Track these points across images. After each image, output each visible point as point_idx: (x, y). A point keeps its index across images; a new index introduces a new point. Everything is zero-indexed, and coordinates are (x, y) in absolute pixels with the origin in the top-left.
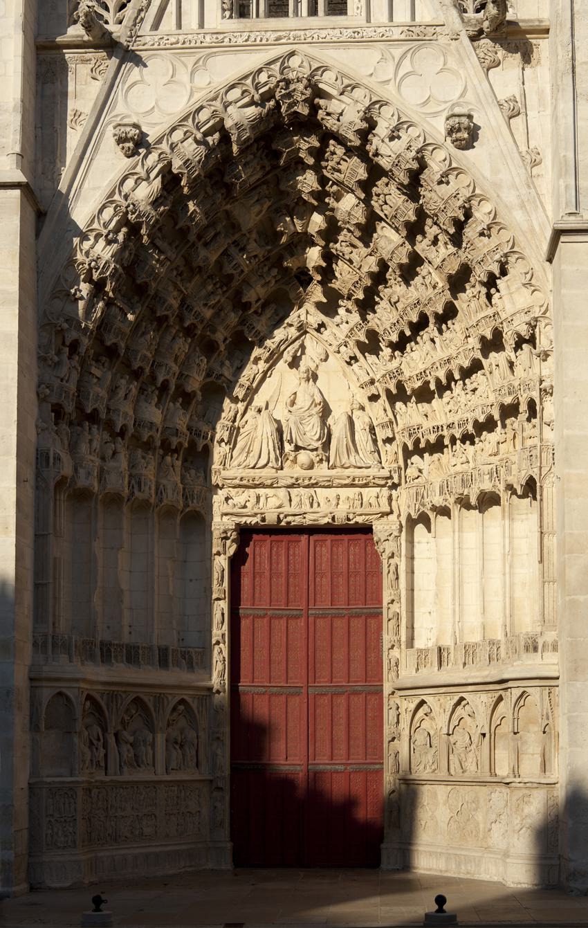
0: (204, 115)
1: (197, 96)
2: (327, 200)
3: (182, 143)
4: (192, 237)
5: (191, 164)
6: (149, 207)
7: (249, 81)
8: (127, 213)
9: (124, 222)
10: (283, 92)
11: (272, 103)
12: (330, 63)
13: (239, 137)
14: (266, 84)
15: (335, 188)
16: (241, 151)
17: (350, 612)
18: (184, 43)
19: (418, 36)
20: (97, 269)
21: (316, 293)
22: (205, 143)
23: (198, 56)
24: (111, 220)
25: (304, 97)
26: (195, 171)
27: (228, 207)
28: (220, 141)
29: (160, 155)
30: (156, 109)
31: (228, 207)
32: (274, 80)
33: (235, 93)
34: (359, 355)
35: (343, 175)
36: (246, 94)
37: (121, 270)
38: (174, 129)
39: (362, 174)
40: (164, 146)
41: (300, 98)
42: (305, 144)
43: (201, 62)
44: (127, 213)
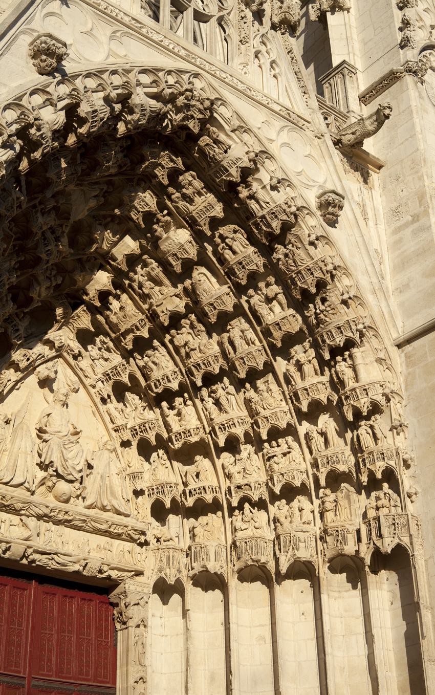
1: (111, 60)
3: (93, 92)
5: (96, 116)
6: (49, 134)
9: (22, 133)
15: (168, 218)
17: (78, 688)
21: (83, 320)
25: (201, 116)
26: (95, 126)
29: (73, 90)
34: (113, 397)
36: (154, 85)
42: (166, 161)
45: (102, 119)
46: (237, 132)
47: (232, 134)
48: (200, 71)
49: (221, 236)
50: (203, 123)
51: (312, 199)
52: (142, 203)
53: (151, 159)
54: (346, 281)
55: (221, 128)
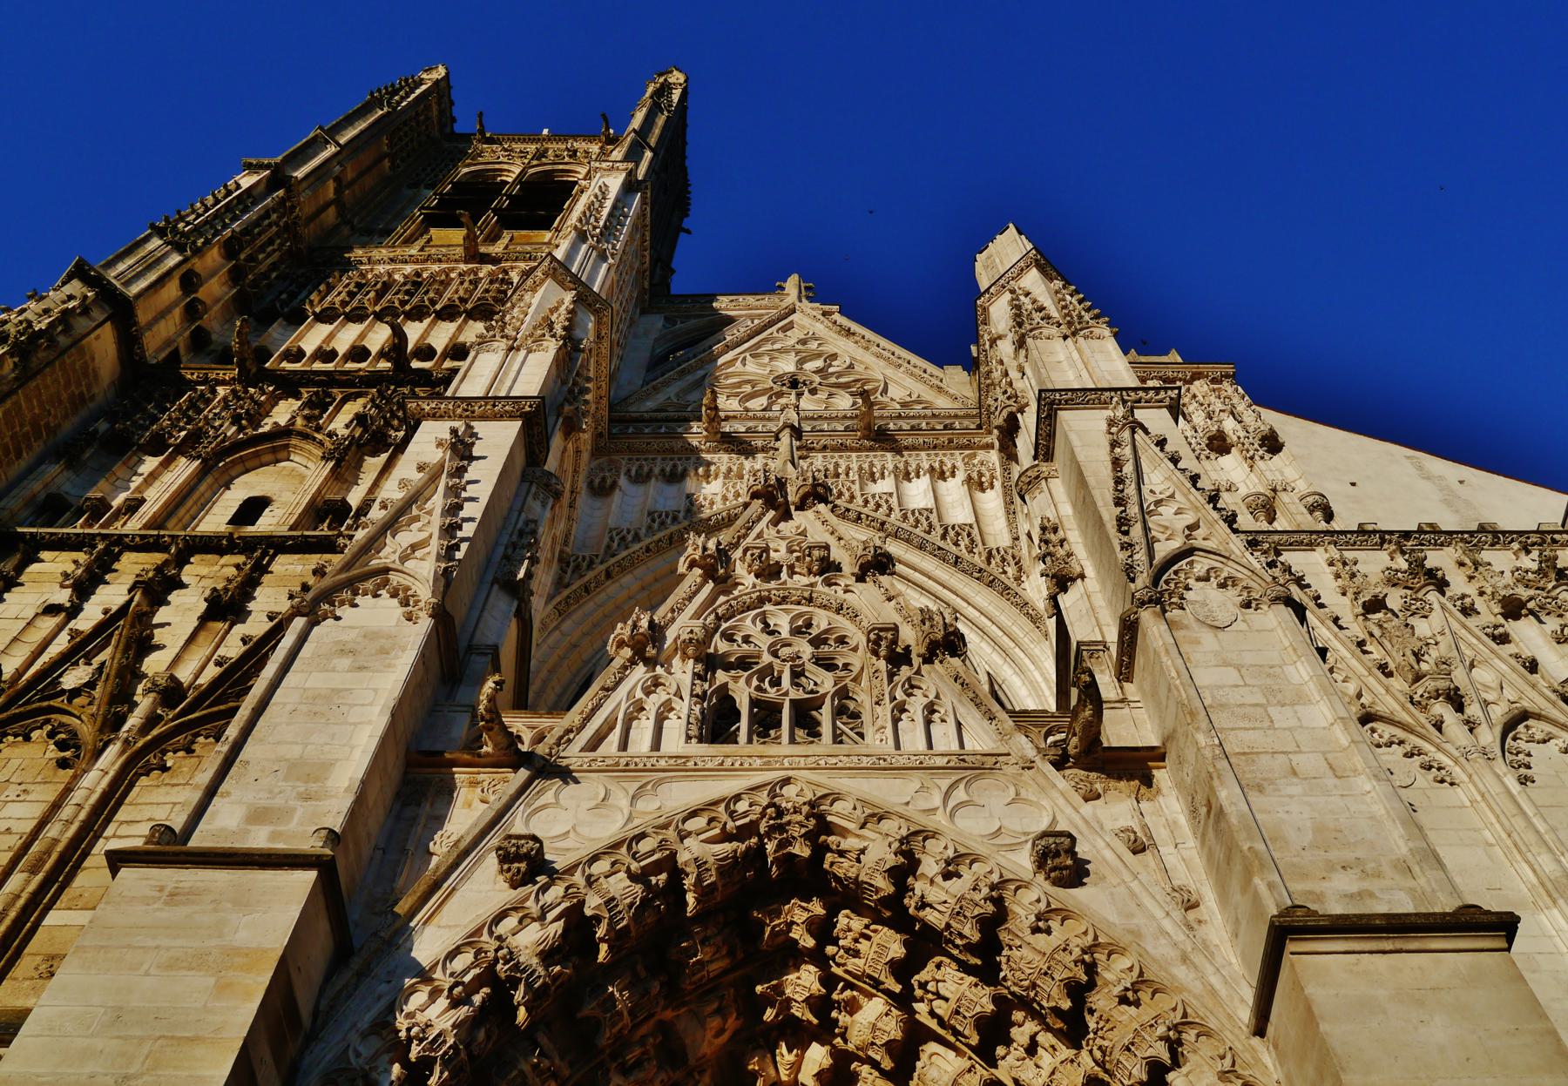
0: (644, 846)
1: (637, 822)
2: (834, 1014)
3: (606, 877)
4: (605, 1038)
5: (617, 906)
6: (535, 961)
7: (722, 808)
8: (496, 960)
9: (488, 976)
10: (772, 822)
11: (754, 840)
12: (844, 790)
13: (699, 879)
14: (745, 814)
15: (848, 993)
16: (701, 916)
18: (627, 764)
19: (971, 767)
20: (421, 1040)
22: (647, 884)
23: (644, 781)
24: (465, 971)
25: (803, 831)
26: (623, 919)
27: (669, 1014)
28: (668, 882)
29: (567, 888)
30: (572, 834)
31: (669, 1014)
32: (758, 809)
33: (699, 823)
35: (863, 961)
37: (463, 1055)
38: (594, 858)
39: (897, 950)
40: (578, 878)
41: (796, 831)
42: (799, 915)
43: (649, 787)
44: (496, 960)
45: (631, 905)
46: (868, 825)
47: (864, 832)
48: (790, 773)
49: (923, 985)
50: (810, 837)
51: (1022, 862)
52: (798, 989)
53: (771, 921)
54: (1122, 963)
55: (844, 832)
